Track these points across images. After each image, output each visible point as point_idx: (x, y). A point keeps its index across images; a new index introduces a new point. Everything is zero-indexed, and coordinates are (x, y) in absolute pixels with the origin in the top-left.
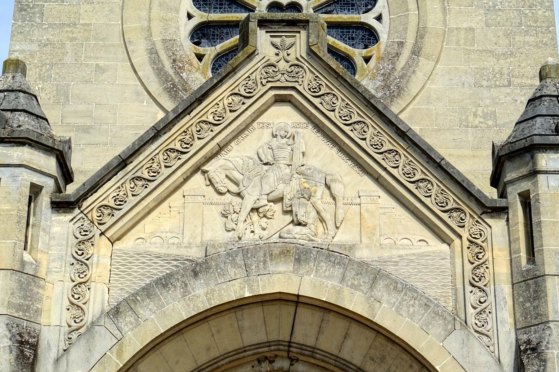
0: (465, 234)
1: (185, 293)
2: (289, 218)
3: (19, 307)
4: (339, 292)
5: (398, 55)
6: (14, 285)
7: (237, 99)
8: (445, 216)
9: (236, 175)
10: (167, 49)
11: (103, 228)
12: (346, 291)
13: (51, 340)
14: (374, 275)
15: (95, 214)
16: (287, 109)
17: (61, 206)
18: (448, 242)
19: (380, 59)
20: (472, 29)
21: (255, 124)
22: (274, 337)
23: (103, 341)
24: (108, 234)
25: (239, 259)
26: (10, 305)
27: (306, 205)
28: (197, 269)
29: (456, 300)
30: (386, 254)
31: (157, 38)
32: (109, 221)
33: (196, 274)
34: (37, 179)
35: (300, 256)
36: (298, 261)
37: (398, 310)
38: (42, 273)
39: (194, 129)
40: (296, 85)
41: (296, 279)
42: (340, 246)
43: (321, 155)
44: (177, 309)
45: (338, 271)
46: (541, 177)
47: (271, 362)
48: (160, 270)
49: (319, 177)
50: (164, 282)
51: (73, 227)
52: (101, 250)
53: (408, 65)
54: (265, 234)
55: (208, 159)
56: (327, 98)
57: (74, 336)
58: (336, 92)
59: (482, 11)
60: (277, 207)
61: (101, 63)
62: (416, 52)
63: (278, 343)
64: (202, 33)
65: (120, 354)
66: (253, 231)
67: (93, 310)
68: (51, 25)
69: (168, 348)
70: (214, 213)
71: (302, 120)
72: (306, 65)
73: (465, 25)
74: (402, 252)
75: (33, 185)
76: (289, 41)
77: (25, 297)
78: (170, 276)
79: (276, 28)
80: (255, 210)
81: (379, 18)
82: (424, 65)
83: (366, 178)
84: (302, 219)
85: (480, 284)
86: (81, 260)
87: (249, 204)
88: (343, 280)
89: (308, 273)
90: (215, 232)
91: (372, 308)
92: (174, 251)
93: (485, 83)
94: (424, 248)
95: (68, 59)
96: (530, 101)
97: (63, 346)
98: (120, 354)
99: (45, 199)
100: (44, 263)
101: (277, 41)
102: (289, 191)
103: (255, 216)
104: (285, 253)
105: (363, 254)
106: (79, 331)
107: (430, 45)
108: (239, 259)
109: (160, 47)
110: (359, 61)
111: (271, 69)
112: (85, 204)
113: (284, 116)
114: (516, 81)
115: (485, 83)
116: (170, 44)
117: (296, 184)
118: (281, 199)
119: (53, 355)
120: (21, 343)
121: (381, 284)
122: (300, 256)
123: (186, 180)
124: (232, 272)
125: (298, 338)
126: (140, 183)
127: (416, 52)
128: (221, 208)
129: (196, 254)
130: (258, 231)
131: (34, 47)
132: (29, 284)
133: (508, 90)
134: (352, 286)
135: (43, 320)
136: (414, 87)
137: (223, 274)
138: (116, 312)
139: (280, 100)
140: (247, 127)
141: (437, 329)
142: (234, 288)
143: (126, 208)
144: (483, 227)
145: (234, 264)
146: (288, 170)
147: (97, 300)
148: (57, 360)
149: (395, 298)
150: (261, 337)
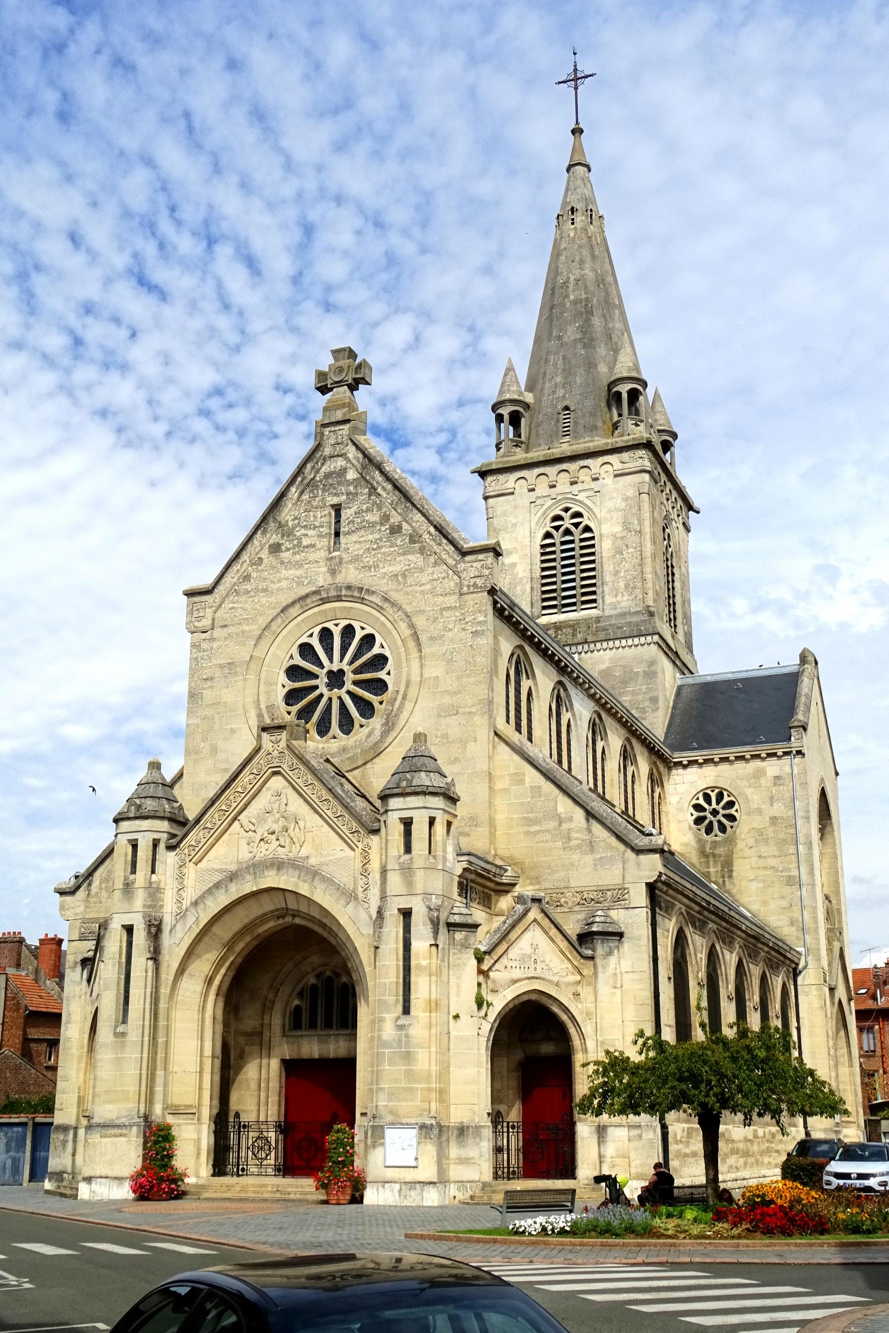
0: (360, 845)
1: (227, 891)
2: (278, 843)
3: (149, 907)
4: (297, 885)
5: (395, 699)
6: (146, 895)
7: (252, 776)
8: (350, 836)
9: (254, 821)
10: (268, 712)
11: (190, 857)
12: (301, 883)
13: (168, 921)
14: (314, 874)
15: (186, 851)
16: (279, 778)
17: (170, 848)
18: (353, 850)
19: (388, 702)
20: (437, 677)
21: (264, 789)
22: (279, 907)
23: (191, 919)
24: (193, 860)
25: (251, 870)
26: (144, 906)
27: (284, 836)
28: (232, 877)
29: (354, 884)
30: (323, 860)
31: (263, 706)
32: (193, 853)
33: (231, 880)
34: (156, 836)
35: (279, 865)
36: (278, 869)
37: (325, 892)
38: (162, 886)
39: (232, 797)
40: (281, 765)
41: (277, 878)
42: (300, 858)
43: (296, 805)
44: (223, 899)
45: (297, 873)
46: (389, 813)
47: (284, 918)
48: (217, 878)
49: (292, 818)
50: (217, 886)
51: (177, 858)
52: (191, 870)
53: (399, 707)
54: (268, 853)
55: (240, 813)
56: (296, 771)
57: (178, 917)
58: (301, 767)
59: (444, 663)
60: (274, 837)
61: (233, 727)
62: (404, 698)
63: (282, 909)
64: (291, 697)
65: (197, 926)
66: (264, 852)
67: (186, 903)
68: (208, 705)
69: (226, 918)
70: (243, 843)
71: (287, 784)
72: (286, 752)
73: (434, 675)
74: (331, 858)
75: (154, 840)
76: (279, 737)
77: (153, 900)
78: (219, 882)
79: (271, 731)
80: (261, 840)
81: (389, 673)
82: (408, 706)
83: (316, 815)
84: (283, 844)
85: (366, 874)
86: (181, 877)
87: (258, 837)
88: (299, 878)
89: (283, 875)
90: (245, 855)
91: (312, 892)
92: (224, 867)
93: (443, 714)
94: (342, 854)
95: (216, 727)
96: (403, 758)
97: (174, 922)
98: (197, 926)
99: (162, 846)
100: (163, 880)
101: (273, 738)
102: (277, 828)
103: (262, 843)
104: (273, 864)
105: (312, 861)
106: (181, 915)
107: (412, 692)
108: (251, 870)
109: (264, 712)
110: (376, 705)
111: (269, 757)
112: (182, 845)
113: (277, 783)
114: (461, 710)
115: (443, 714)
116: (270, 708)
117: (282, 822)
118: (273, 833)
119: (169, 928)
120: (149, 925)
121: (317, 878)
122: (279, 865)
123: (230, 825)
124: (248, 877)
125: (290, 906)
126: (207, 831)
127: (404, 698)
128: (247, 840)
129: (233, 868)
130: (264, 852)
131: (198, 721)
132: (155, 893)
133: (456, 717)
134: (305, 881)
135: (164, 910)
136: (401, 723)
137: (243, 879)
138: (195, 904)
139: (275, 773)
140: (259, 791)
141: (343, 902)
142: (249, 887)
143: (200, 845)
144: (369, 840)
145: (249, 873)
146: (278, 815)
147: (190, 895)
148: (171, 930)
149: (323, 886)
150: (272, 907)
